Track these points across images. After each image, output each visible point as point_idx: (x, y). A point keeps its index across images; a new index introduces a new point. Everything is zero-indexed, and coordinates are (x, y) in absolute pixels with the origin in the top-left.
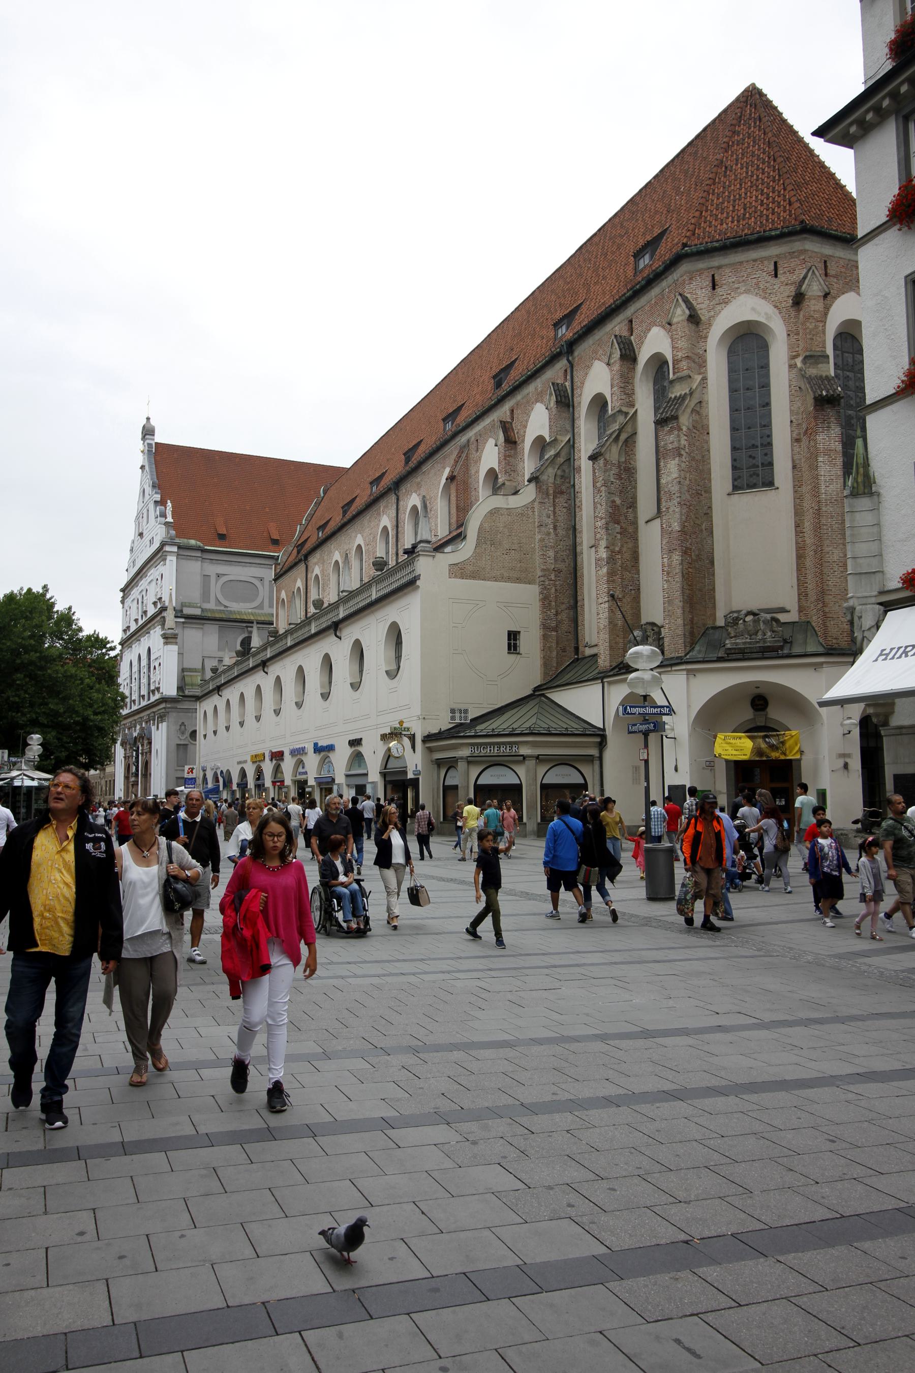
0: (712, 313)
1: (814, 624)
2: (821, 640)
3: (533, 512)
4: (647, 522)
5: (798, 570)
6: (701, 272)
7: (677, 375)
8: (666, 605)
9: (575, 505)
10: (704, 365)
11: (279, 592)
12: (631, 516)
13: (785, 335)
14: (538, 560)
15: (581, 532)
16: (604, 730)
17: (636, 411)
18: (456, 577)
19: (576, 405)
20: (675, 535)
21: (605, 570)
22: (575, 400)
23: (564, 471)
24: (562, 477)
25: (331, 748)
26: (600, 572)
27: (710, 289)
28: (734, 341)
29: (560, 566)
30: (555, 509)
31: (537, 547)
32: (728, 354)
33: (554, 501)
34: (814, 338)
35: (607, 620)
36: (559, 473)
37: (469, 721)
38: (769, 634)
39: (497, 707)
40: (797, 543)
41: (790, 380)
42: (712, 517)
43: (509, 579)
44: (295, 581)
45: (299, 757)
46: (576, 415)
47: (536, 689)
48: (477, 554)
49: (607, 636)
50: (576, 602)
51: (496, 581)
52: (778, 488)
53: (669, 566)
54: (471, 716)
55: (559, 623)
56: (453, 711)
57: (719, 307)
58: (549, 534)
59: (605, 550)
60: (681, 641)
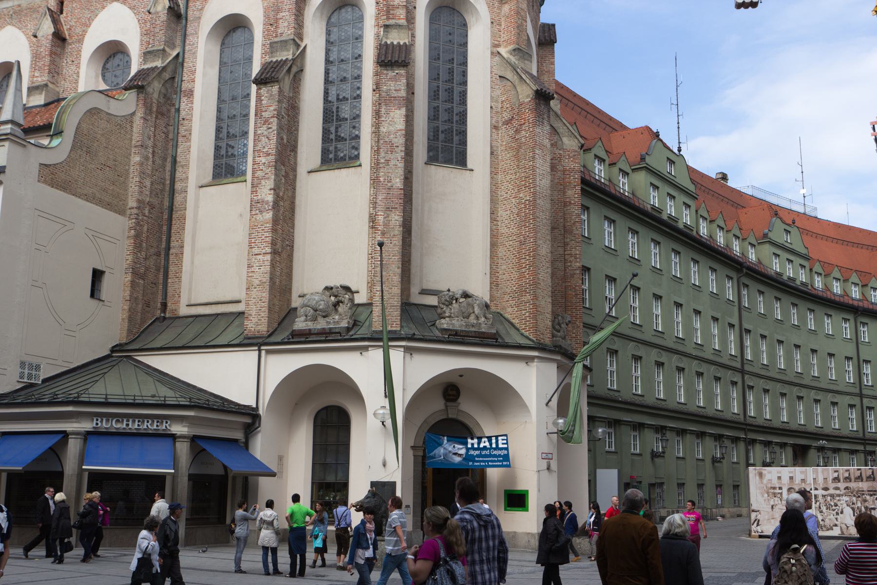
1: (507, 316)
2: (527, 334)
3: (132, 127)
4: (309, 172)
5: (492, 257)
7: (391, 22)
9: (178, 133)
10: (412, 21)
14: (133, 187)
15: (186, 166)
17: (305, 47)
18: (45, 182)
19: (190, 18)
21: (269, 215)
22: (190, 13)
23: (167, 90)
24: (165, 96)
26: (259, 217)
28: (434, 10)
29: (155, 201)
30: (155, 130)
32: (430, 20)
33: (156, 122)
34: (521, 33)
35: (267, 276)
36: (163, 91)
37: (40, 383)
38: (483, 319)
40: (491, 230)
41: (492, 67)
43: (100, 202)
46: (190, 30)
47: (113, 350)
48: (70, 160)
49: (266, 295)
50: (168, 248)
52: (472, 170)
53: (386, 225)
55: (147, 269)
56: (23, 364)
58: (147, 158)
59: (272, 192)
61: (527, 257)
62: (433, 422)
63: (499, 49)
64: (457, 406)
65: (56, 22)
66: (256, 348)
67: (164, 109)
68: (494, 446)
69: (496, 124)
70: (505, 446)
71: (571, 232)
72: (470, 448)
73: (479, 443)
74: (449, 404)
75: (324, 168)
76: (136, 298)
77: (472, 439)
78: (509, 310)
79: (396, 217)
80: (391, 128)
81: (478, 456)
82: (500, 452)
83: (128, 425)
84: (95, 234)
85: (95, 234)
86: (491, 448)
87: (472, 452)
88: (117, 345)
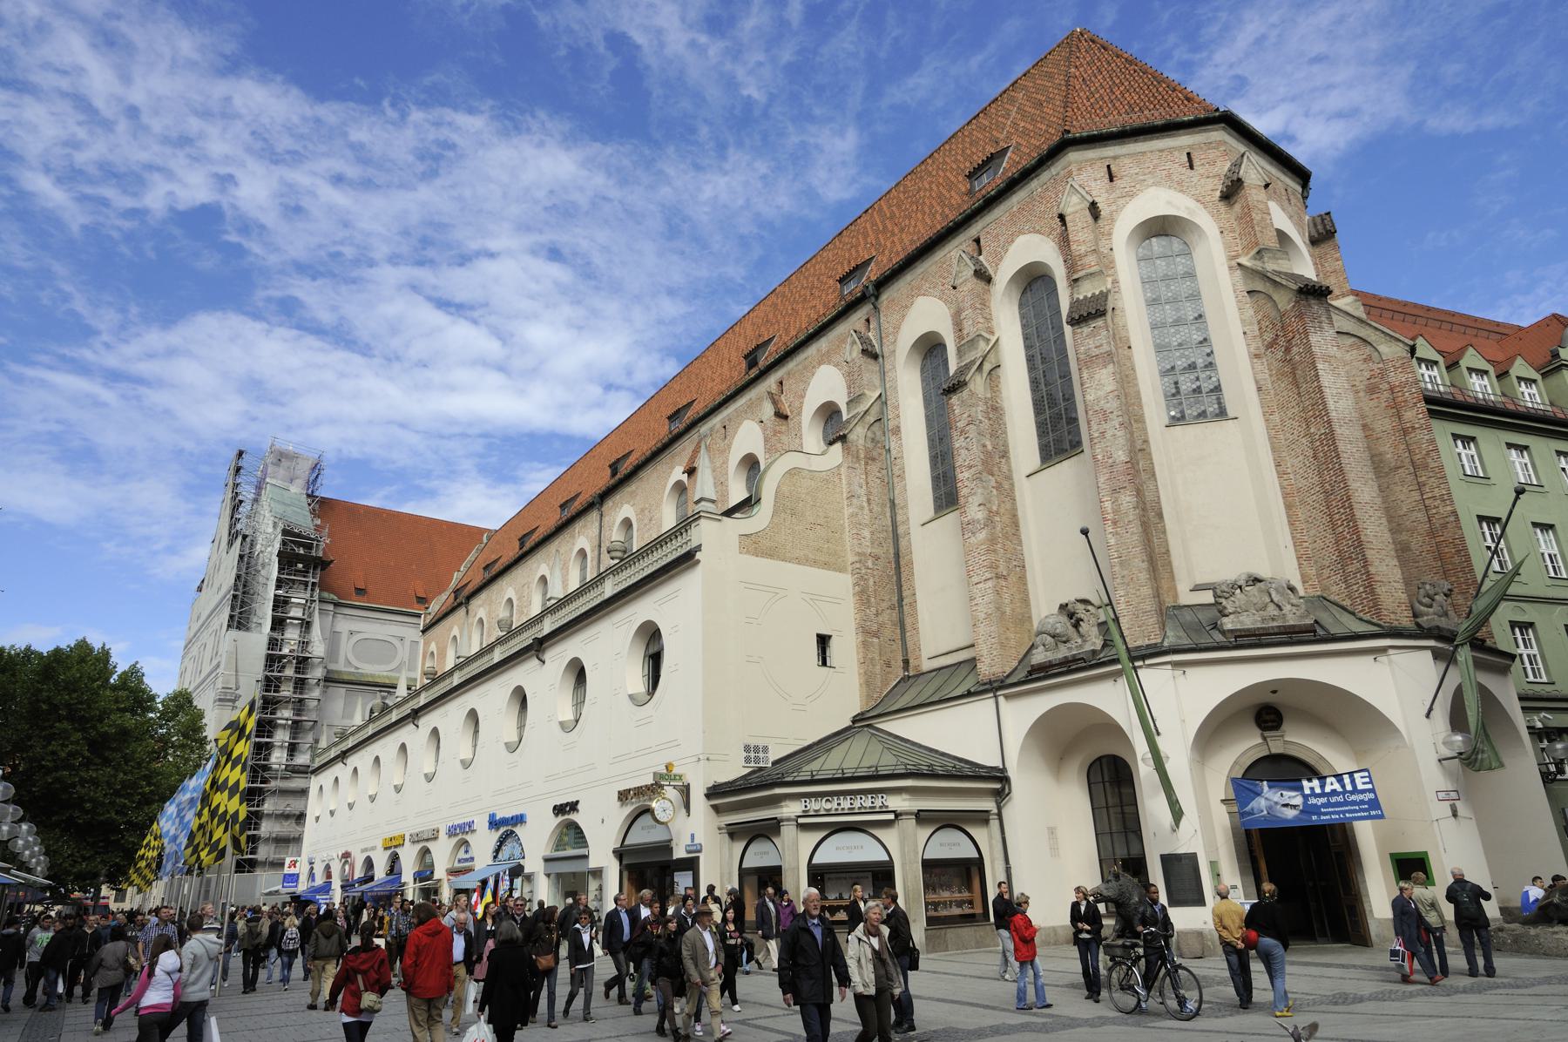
0: (1115, 208)
1: (1332, 598)
2: (1367, 617)
6: (1092, 162)
8: (1116, 569)
11: (427, 644)
12: (1005, 468)
13: (1218, 233)
16: (1004, 770)
18: (748, 552)
19: (886, 354)
20: (1121, 468)
22: (885, 349)
25: (519, 820)
26: (973, 540)
27: (1106, 179)
31: (846, 525)
37: (770, 765)
38: (1289, 607)
39: (806, 744)
40: (1282, 488)
41: (1234, 285)
42: (1150, 454)
43: (815, 563)
44: (451, 629)
45: (460, 837)
46: (888, 367)
50: (901, 599)
51: (799, 563)
53: (1115, 512)
54: (775, 754)
56: (747, 748)
57: (1121, 201)
58: (862, 508)
60: (1153, 620)
61: (1342, 510)
62: (1249, 763)
63: (1240, 261)
64: (1282, 736)
65: (775, 403)
66: (992, 695)
67: (875, 454)
68: (1349, 787)
69: (1257, 352)
70: (1370, 786)
71: (1426, 467)
72: (1308, 795)
73: (1323, 786)
74: (1267, 734)
75: (1045, 466)
76: (872, 659)
77: (1310, 780)
78: (1335, 588)
79: (1128, 499)
80: (1100, 393)
81: (1324, 805)
82: (1361, 797)
83: (839, 804)
84: (812, 597)
85: (812, 597)
86: (1345, 792)
87: (1313, 801)
88: (858, 714)
